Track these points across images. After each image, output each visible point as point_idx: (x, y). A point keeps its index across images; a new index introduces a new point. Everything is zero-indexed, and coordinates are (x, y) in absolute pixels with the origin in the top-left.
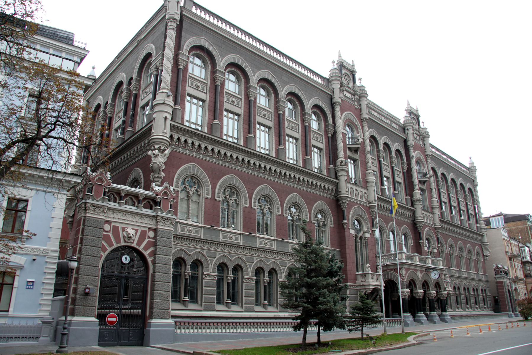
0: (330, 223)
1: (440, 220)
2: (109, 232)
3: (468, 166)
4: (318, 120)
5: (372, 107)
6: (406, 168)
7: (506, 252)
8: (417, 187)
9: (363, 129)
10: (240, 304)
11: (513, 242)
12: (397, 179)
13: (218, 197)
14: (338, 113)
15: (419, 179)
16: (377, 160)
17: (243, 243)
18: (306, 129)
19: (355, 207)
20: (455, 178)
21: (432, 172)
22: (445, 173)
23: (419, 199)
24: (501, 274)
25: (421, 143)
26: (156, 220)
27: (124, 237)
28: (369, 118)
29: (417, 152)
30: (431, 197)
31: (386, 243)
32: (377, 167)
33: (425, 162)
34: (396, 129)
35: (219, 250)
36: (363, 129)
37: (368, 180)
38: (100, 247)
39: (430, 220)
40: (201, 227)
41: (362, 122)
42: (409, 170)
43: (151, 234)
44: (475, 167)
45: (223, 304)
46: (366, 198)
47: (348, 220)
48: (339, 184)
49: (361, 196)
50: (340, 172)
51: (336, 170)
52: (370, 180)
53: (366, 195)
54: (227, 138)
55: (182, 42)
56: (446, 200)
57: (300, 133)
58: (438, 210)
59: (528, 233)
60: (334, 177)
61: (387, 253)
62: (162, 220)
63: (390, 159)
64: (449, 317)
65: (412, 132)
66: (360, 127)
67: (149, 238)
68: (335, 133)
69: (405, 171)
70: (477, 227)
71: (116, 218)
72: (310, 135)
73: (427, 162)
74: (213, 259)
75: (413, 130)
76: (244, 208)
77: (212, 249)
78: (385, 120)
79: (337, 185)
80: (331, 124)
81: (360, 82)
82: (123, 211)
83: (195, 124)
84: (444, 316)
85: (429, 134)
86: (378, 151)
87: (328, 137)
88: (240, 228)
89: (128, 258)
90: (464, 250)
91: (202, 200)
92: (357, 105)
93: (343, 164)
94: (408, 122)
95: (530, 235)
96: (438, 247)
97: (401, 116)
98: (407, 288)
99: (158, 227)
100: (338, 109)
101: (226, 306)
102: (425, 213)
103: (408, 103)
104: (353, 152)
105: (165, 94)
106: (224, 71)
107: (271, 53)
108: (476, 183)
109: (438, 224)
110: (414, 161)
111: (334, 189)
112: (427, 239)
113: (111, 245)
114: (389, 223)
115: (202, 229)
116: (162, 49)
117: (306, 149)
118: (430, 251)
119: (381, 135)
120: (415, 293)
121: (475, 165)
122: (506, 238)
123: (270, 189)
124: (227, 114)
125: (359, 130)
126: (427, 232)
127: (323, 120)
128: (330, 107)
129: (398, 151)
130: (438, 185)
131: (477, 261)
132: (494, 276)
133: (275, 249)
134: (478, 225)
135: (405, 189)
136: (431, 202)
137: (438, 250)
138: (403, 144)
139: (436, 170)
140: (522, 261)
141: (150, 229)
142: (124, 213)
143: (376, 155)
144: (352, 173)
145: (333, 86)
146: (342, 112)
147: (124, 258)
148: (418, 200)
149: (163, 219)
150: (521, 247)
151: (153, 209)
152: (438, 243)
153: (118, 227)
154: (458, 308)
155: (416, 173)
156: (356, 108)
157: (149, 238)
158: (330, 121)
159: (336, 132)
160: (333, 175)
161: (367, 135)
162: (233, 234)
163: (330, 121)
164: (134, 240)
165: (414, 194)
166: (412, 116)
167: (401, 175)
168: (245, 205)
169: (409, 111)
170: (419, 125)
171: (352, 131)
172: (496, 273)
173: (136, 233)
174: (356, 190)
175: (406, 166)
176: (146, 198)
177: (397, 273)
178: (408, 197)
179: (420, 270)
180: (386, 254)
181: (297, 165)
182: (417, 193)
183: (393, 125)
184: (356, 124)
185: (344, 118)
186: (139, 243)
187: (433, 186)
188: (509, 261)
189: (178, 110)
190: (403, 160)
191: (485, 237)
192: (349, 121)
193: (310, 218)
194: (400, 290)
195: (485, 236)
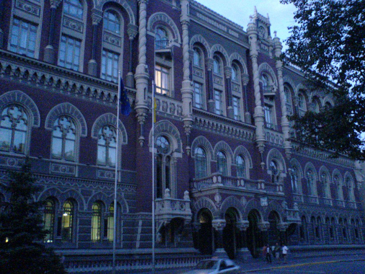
28: (191, 20)
34: (236, 38)
39: (277, 140)
42: (251, 83)
49: (170, 109)
57: (84, 34)
80: (132, 26)
104: (164, 58)
106: (101, 10)
120: (239, 224)
138: (245, 55)
174: (163, 102)
178: (248, 113)
181: (106, 80)
182: (259, 109)
193: (42, 124)
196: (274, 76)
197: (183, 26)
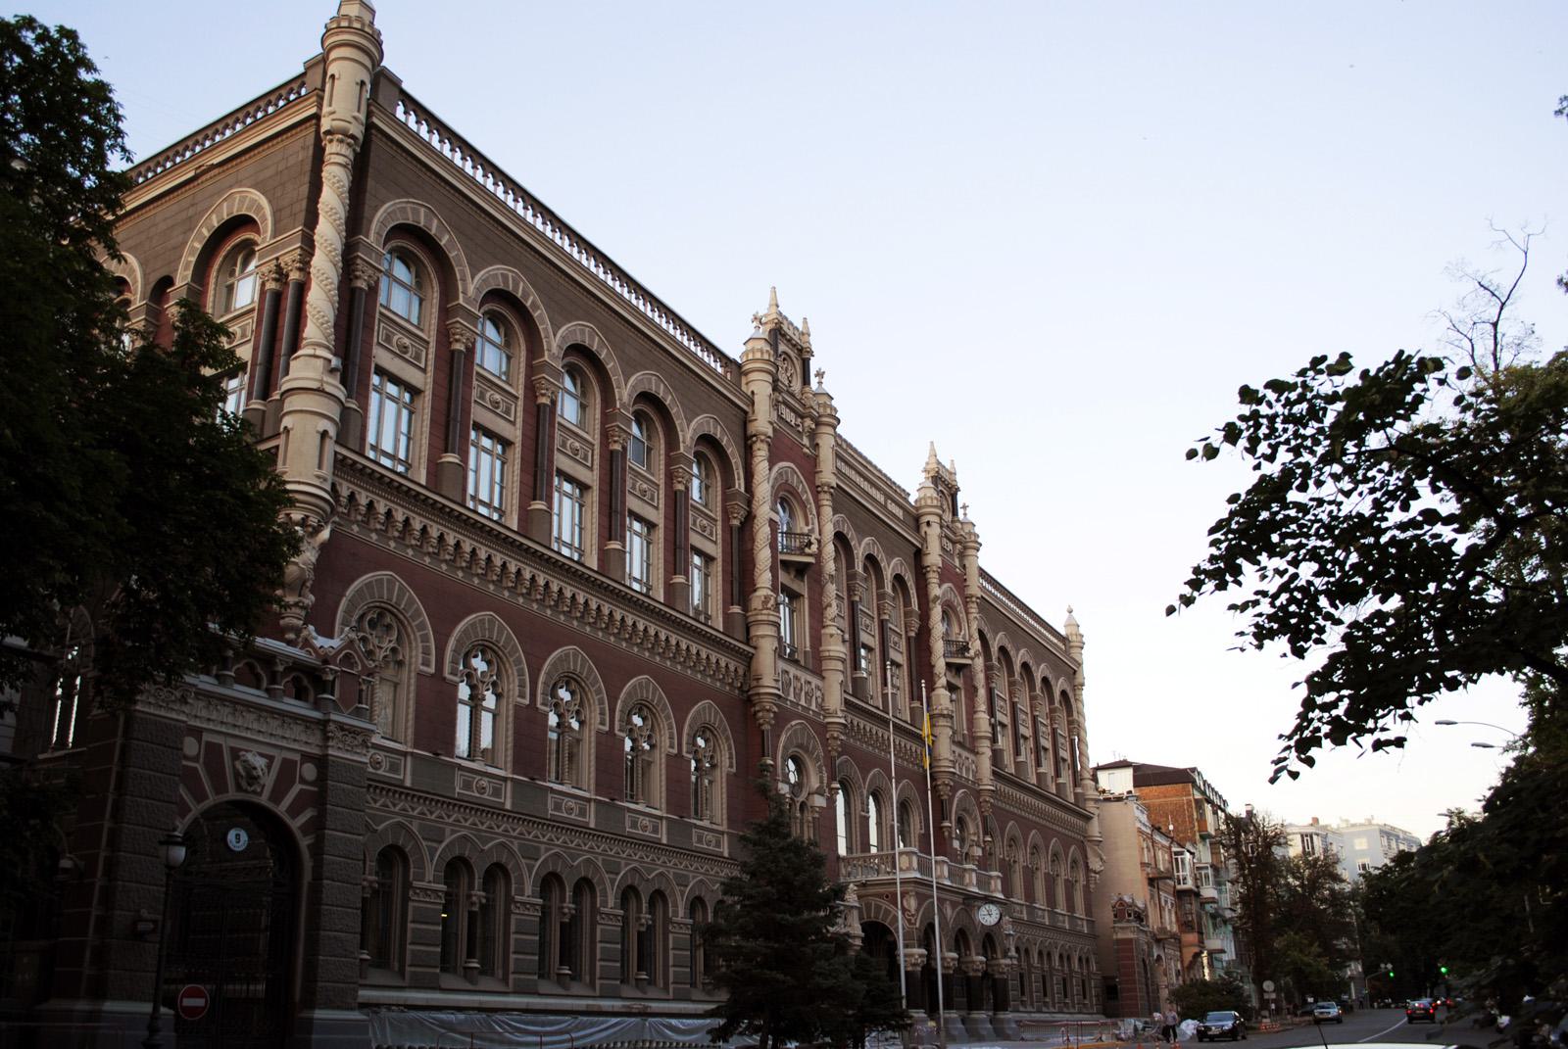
0: (726, 761)
1: (994, 773)
2: (196, 759)
3: (1063, 632)
4: (707, 476)
5: (846, 454)
6: (917, 626)
7: (1143, 864)
8: (943, 681)
9: (819, 514)
10: (500, 973)
11: (1157, 838)
12: (893, 655)
13: (451, 674)
14: (761, 466)
15: (949, 660)
16: (846, 601)
17: (513, 804)
18: (677, 502)
19: (793, 723)
20: (1031, 663)
21: (978, 642)
22: (1009, 647)
23: (945, 712)
24: (1128, 921)
25: (957, 563)
26: (325, 732)
27: (237, 774)
29: (946, 586)
30: (972, 710)
31: (861, 824)
32: (846, 618)
33: (963, 615)
34: (898, 519)
35: (451, 820)
36: (819, 514)
37: (827, 654)
38: (176, 803)
39: (968, 770)
40: (405, 754)
41: (819, 492)
42: (925, 632)
43: (309, 771)
45: (454, 971)
46: (820, 700)
47: (774, 759)
48: (754, 660)
49: (806, 693)
50: (762, 627)
51: (751, 619)
52: (832, 654)
53: (819, 694)
54: (475, 506)
55: (366, 207)
56: (1007, 720)
58: (987, 743)
59: (1191, 816)
60: (745, 640)
61: (862, 852)
62: (339, 734)
63: (878, 600)
64: (1014, 1025)
65: (938, 530)
67: (303, 781)
68: (750, 518)
69: (913, 634)
70: (1076, 794)
71: (216, 724)
72: (687, 519)
73: (967, 613)
74: (435, 845)
75: (941, 527)
76: (517, 707)
77: (433, 817)
78: (873, 492)
79: (748, 659)
81: (820, 383)
82: (235, 702)
83: (393, 457)
84: (1002, 1021)
85: (979, 540)
86: (852, 576)
87: (731, 527)
88: (506, 763)
89: (244, 837)
91: (409, 678)
92: (808, 444)
93: (769, 606)
94: (929, 502)
96: (985, 842)
97: (912, 482)
98: (919, 947)
99: (330, 752)
100: (761, 453)
101: (465, 977)
102: (958, 750)
103: (933, 449)
105: (320, 363)
107: (591, 265)
108: (1078, 680)
109: (987, 782)
110: (937, 612)
111: (741, 672)
112: (961, 822)
113: (200, 797)
114: (869, 772)
115: (409, 759)
116: (302, 217)
117: (677, 555)
118: (965, 851)
119: (862, 533)
121: (1082, 630)
122: (1144, 829)
123: (583, 659)
124: (477, 436)
125: (810, 516)
126: (960, 800)
127: (719, 478)
128: (742, 443)
129: (898, 579)
130: (988, 679)
131: (1070, 886)
132: (1112, 925)
133: (592, 825)
134: (1079, 790)
136: (971, 722)
137: (983, 849)
138: (912, 561)
139: (988, 636)
141: (307, 757)
142: (239, 707)
143: (845, 585)
144: (786, 632)
146: (772, 461)
147: (231, 835)
148: (944, 716)
149: (343, 729)
150: (1177, 853)
151: (311, 698)
152: (986, 833)
153: (221, 745)
154: (1023, 1003)
157: (303, 781)
158: (740, 485)
159: (755, 517)
160: (740, 634)
161: (829, 531)
162: (487, 779)
163: (740, 485)
164: (263, 786)
166: (940, 488)
167: (903, 643)
168: (519, 699)
169: (932, 474)
170: (955, 513)
171: (792, 515)
172: (1116, 916)
173: (269, 767)
174: (796, 678)
175: (916, 623)
176: (297, 666)
177: (896, 905)
179: (951, 902)
183: (892, 507)
184: (804, 498)
185: (776, 479)
186: (277, 795)
187: (980, 678)
188: (1147, 888)
189: (352, 412)
191: (1095, 821)
192: (787, 487)
194: (902, 951)
195: (1096, 819)
196: (963, 615)
197: (758, 445)
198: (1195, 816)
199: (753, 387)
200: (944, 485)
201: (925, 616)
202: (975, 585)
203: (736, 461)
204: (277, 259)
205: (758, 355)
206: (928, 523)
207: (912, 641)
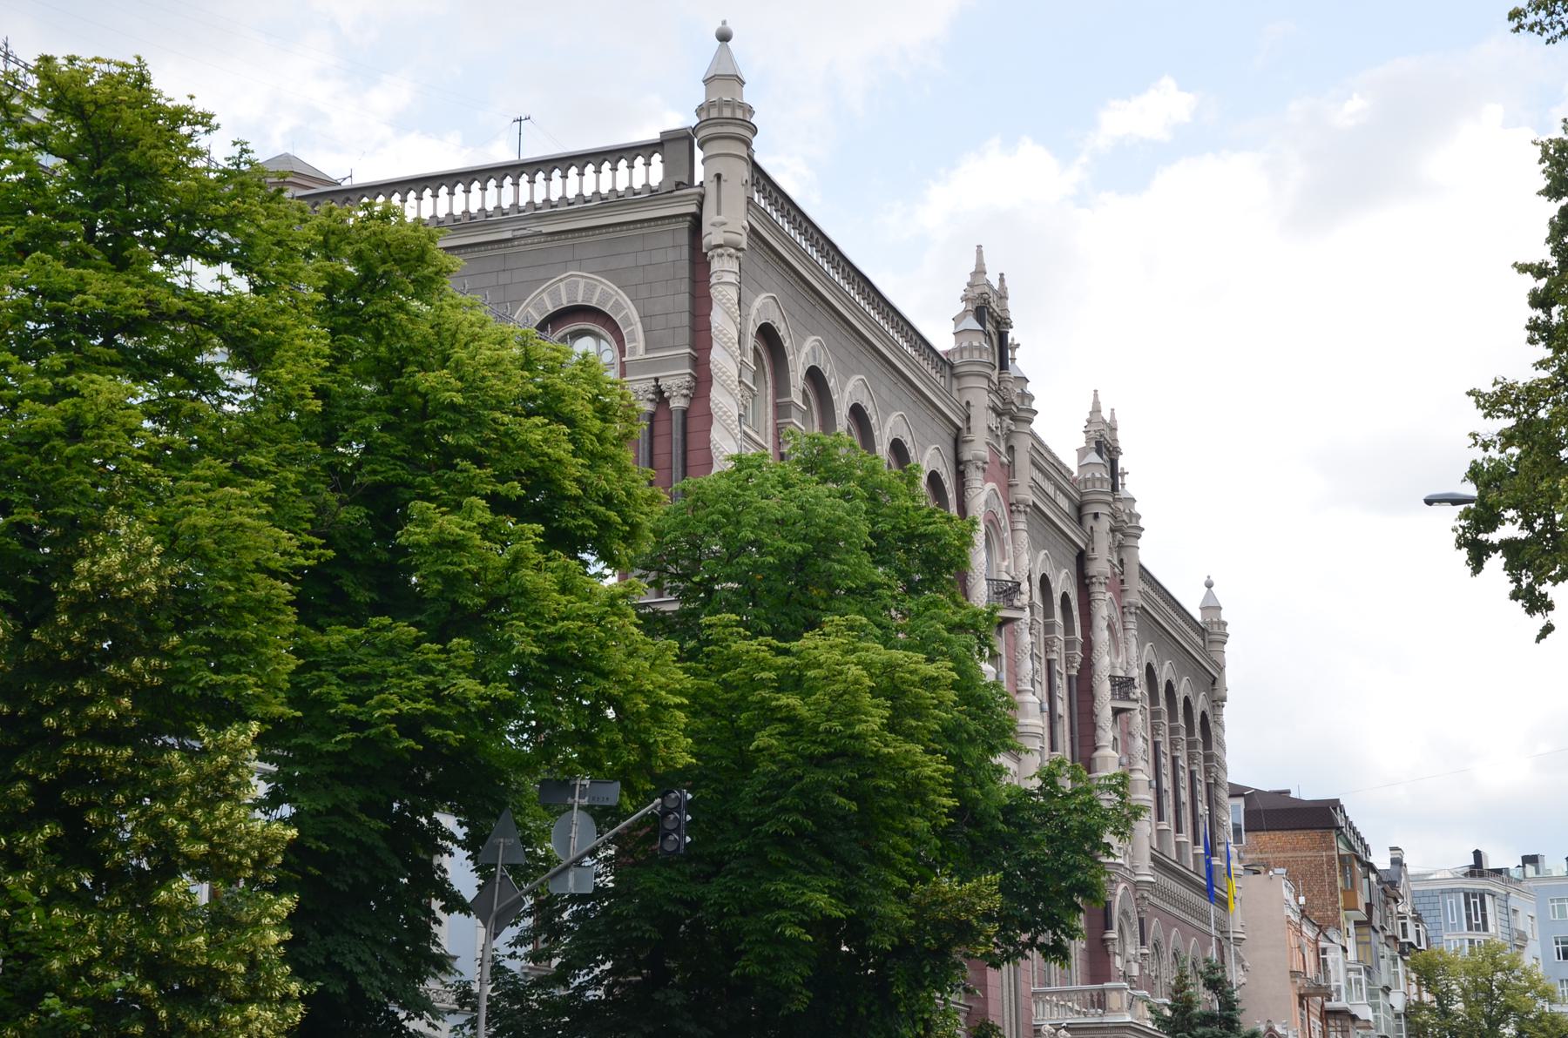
1: (1153, 858)
3: (1198, 616)
6: (1079, 660)
7: (1294, 974)
42: (1088, 666)
44: (1225, 624)
52: (1029, 729)
59: (1333, 883)
66: (1007, 535)
69: (1074, 672)
85: (1142, 523)
90: (1164, 949)
95: (1340, 896)
108: (1217, 694)
121: (1224, 616)
129: (1065, 597)
135: (1072, 740)
138: (1074, 568)
140: (1323, 1005)
145: (969, 396)
150: (1324, 951)
155: (1107, 685)
156: (1002, 464)
165: (1098, 762)
180: (1059, 988)
190: (1053, 616)
198: (1340, 883)
199: (968, 396)
200: (1104, 445)
201: (1088, 646)
202: (1135, 593)
203: (951, 496)
204: (657, 380)
205: (976, 357)
206: (1096, 516)
207: (1074, 681)
